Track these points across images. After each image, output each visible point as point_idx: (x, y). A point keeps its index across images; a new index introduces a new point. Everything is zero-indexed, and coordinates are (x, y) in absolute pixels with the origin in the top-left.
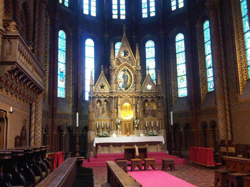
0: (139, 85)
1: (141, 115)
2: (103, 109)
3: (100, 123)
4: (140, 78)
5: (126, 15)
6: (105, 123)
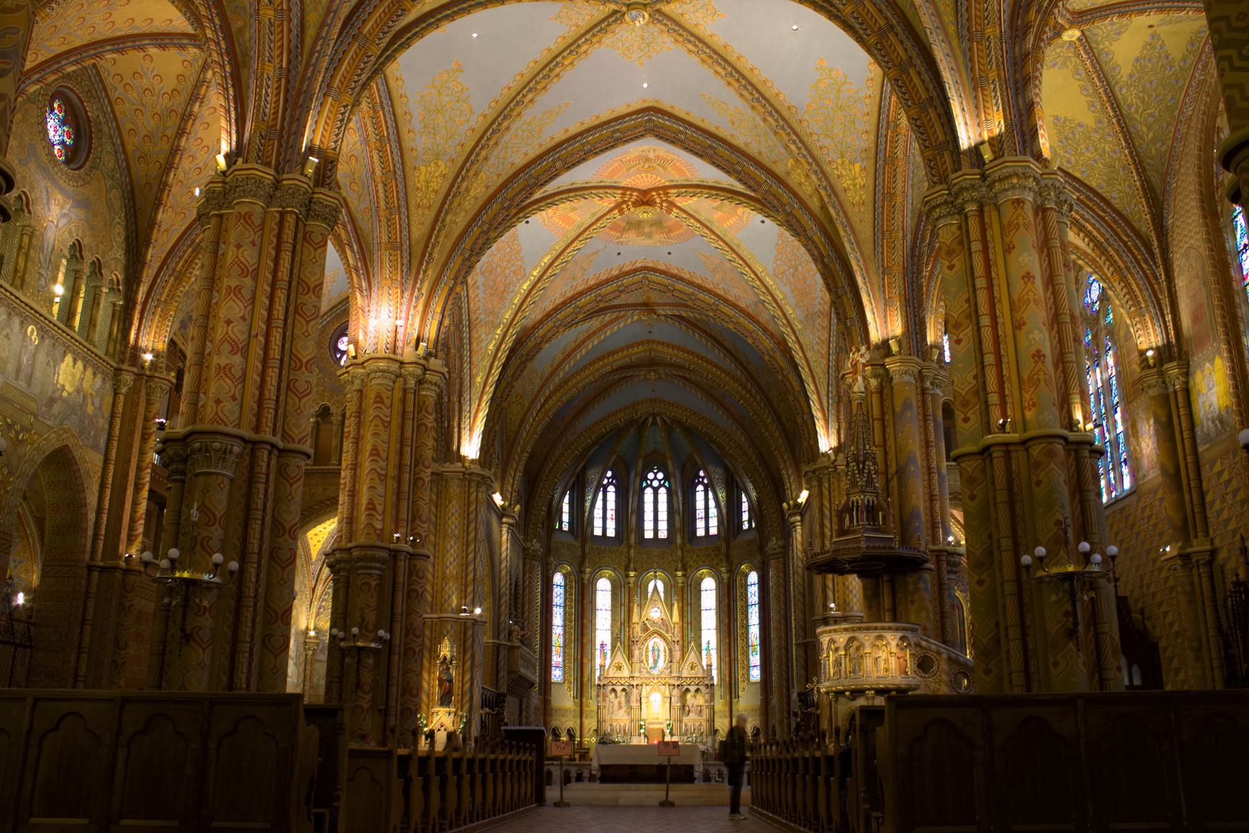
0: (675, 666)
1: (676, 713)
2: (620, 703)
3: (614, 724)
4: (677, 654)
5: (669, 530)
6: (622, 724)
